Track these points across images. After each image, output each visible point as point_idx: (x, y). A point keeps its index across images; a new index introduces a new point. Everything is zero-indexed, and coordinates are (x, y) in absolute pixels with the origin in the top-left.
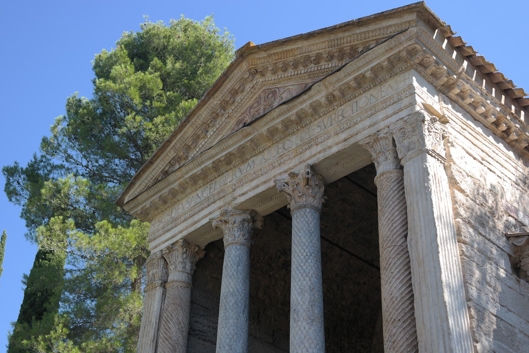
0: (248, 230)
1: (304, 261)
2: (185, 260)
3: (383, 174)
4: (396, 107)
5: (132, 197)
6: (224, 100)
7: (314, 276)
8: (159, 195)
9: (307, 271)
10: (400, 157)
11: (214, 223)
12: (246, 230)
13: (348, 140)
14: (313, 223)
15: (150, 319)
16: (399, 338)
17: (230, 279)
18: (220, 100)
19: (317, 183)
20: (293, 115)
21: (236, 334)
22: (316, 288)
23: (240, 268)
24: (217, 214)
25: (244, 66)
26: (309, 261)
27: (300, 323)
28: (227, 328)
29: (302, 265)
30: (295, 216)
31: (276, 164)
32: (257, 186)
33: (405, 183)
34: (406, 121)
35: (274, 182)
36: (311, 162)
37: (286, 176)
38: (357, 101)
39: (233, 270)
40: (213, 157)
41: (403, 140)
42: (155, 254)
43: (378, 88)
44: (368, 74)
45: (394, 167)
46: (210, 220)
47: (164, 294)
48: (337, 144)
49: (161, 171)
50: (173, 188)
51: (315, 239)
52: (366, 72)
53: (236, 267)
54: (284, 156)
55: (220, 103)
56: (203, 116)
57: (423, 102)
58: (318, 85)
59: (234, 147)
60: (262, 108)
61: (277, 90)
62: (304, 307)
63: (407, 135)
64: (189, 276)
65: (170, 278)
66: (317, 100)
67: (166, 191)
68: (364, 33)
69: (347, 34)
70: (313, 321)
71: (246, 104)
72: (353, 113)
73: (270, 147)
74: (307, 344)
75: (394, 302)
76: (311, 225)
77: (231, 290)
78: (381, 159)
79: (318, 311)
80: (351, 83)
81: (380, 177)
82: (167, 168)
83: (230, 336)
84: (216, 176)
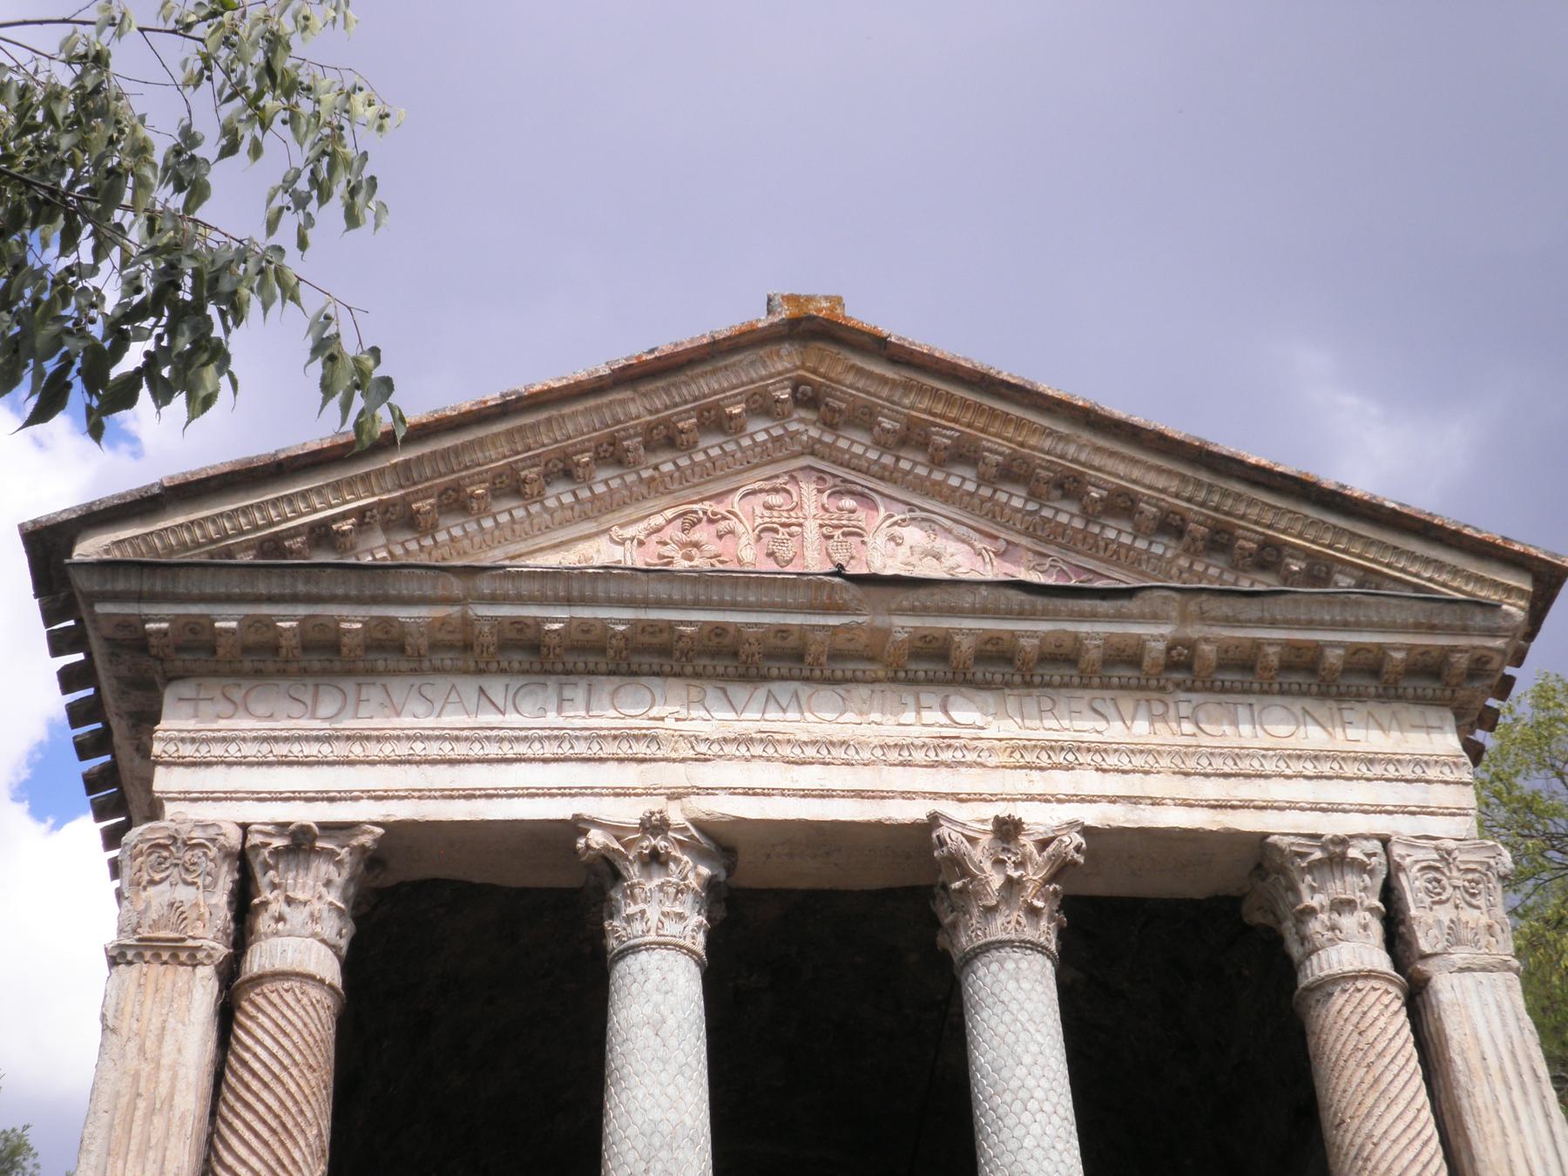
5: (129, 554)
8: (302, 610)
11: (597, 838)
17: (680, 1079)
18: (657, 411)
20: (1033, 635)
24: (629, 813)
25: (786, 360)
34: (1449, 853)
36: (1093, 816)
38: (1251, 705)
39: (687, 1048)
40: (646, 604)
41: (1434, 903)
43: (1333, 705)
44: (1334, 657)
46: (577, 818)
48: (1187, 804)
58: (1166, 597)
59: (753, 618)
63: (1444, 897)
73: (875, 681)
80: (1271, 650)
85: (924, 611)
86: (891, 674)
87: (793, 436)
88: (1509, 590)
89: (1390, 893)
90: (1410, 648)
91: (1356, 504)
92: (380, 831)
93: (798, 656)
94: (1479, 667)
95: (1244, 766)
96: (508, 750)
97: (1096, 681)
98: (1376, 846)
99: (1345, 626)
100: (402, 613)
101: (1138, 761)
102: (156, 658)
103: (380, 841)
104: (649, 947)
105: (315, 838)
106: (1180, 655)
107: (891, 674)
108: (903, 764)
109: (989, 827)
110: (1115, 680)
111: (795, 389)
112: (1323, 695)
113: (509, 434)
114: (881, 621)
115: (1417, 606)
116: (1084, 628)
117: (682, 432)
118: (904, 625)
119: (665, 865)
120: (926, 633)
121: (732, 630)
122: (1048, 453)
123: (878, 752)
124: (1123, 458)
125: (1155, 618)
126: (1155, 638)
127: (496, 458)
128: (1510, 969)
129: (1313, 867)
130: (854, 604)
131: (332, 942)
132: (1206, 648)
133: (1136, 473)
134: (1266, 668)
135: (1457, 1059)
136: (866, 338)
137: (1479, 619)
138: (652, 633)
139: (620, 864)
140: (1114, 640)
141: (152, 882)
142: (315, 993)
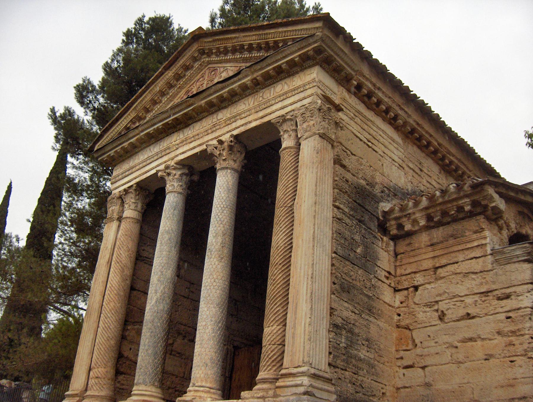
0: (185, 182)
1: (221, 211)
2: (137, 201)
3: (285, 149)
4: (302, 95)
5: (100, 147)
6: (177, 73)
7: (227, 224)
8: (120, 147)
9: (222, 219)
10: (299, 136)
11: (160, 174)
12: (184, 182)
13: (264, 118)
14: (232, 182)
15: (107, 245)
16: (278, 278)
19: (239, 150)
20: (225, 93)
21: (168, 263)
22: (228, 233)
23: (175, 211)
24: (162, 167)
25: (195, 47)
26: (225, 212)
27: (212, 259)
28: (161, 258)
29: (219, 214)
30: (219, 174)
31: (210, 131)
32: (194, 148)
33: (300, 158)
35: (206, 146)
36: (235, 133)
37: (215, 142)
39: (170, 213)
41: (303, 123)
42: (115, 194)
44: (284, 66)
45: (295, 144)
46: (157, 171)
47: (119, 226)
48: (256, 120)
49: (124, 127)
50: (131, 142)
51: (232, 194)
52: (283, 64)
53: (172, 211)
54: (216, 125)
55: (174, 76)
56: (160, 85)
57: (324, 94)
60: (205, 82)
61: (218, 69)
62: (217, 247)
64: (140, 214)
65: (125, 215)
66: (244, 83)
67: (126, 144)
68: (285, 32)
69: (272, 31)
70: (222, 258)
71: (194, 78)
72: (270, 96)
73: (207, 116)
74: (215, 276)
75: (278, 250)
76: (230, 183)
77: (167, 229)
78: (286, 136)
79: (227, 252)
80: (271, 72)
81: (283, 150)
82: (129, 125)
83: (163, 264)
84: (165, 135)
85: (204, 98)
88: (317, 28)
92: (135, 185)
93: (190, 118)
95: (268, 104)
96: (151, 160)
100: (132, 140)
101: (248, 113)
105: (127, 190)
108: (207, 134)
110: (247, 94)
112: (289, 76)
113: (149, 92)
114: (200, 104)
115: (297, 44)
116: (234, 86)
117: (180, 74)
122: (237, 42)
125: (246, 76)
126: (247, 81)
127: (149, 97)
128: (316, 134)
129: (281, 125)
130: (193, 102)
137: (311, 40)
142: (128, 220)
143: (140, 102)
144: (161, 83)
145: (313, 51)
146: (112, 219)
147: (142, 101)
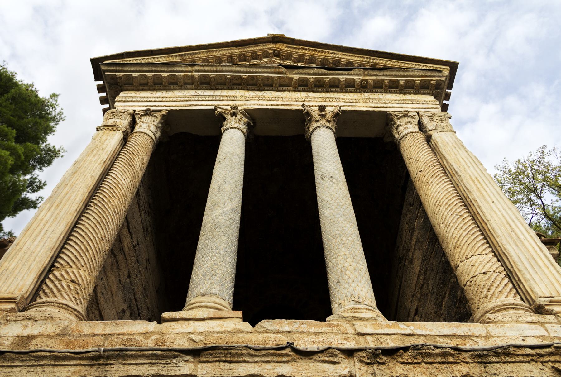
6: (244, 54)
50: (175, 75)
80: (386, 81)
85: (302, 74)
86: (294, 89)
87: (274, 61)
89: (421, 127)
90: (421, 80)
91: (405, 57)
92: (167, 111)
94: (439, 85)
97: (344, 90)
98: (416, 114)
99: (404, 76)
102: (119, 86)
103: (167, 113)
104: (231, 128)
106: (364, 83)
107: (294, 89)
109: (317, 108)
111: (274, 52)
113: (206, 52)
114: (291, 76)
115: (422, 72)
116: (340, 77)
117: (247, 56)
118: (296, 77)
119: (236, 116)
120: (302, 79)
121: (255, 78)
123: (290, 99)
124: (349, 56)
125: (357, 75)
129: (399, 118)
131: (154, 132)
132: (370, 81)
133: (352, 58)
134: (386, 86)
135: (441, 145)
136: (289, 40)
137: (437, 74)
138: (237, 80)
139: (226, 116)
140: (348, 80)
141: (110, 119)
143: (191, 54)
144: (224, 52)
145: (436, 82)
146: (115, 129)
147: (194, 54)
